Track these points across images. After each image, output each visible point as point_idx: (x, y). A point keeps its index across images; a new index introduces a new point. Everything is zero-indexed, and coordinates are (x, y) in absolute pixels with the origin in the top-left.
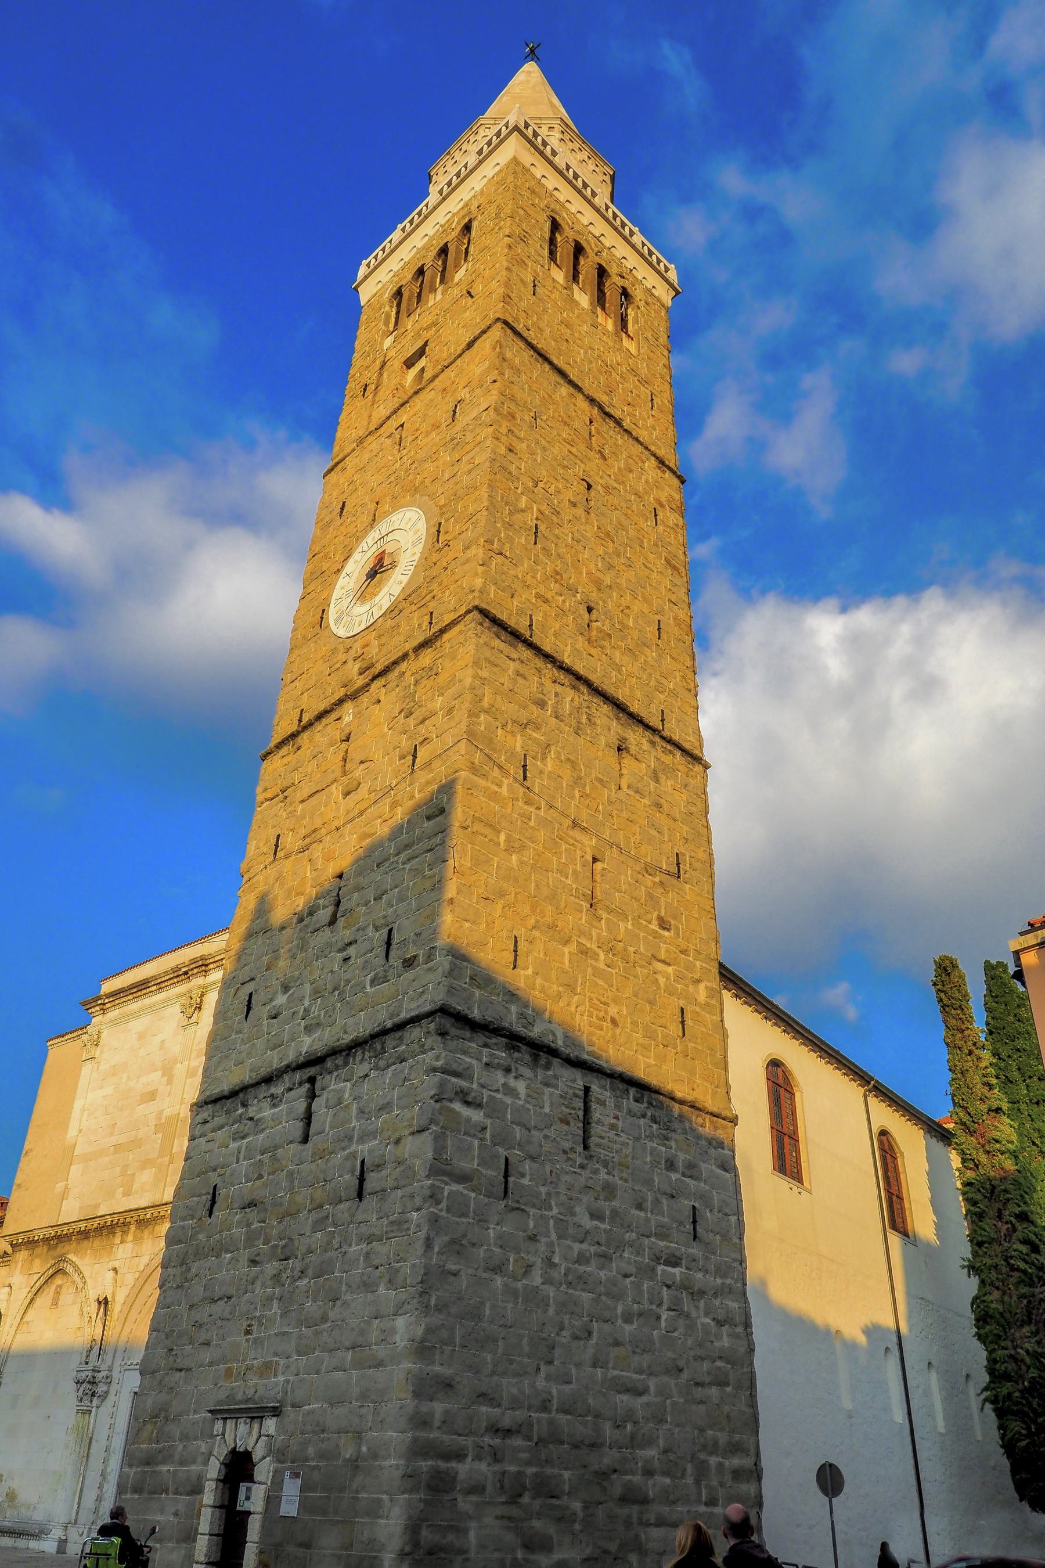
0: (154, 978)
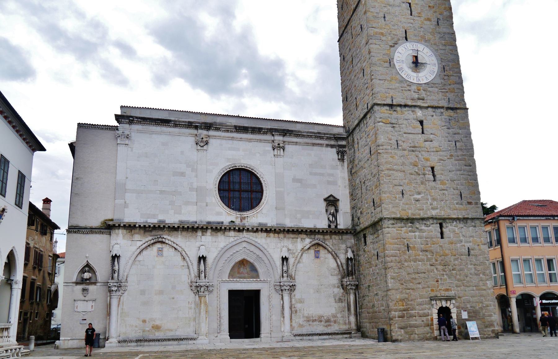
0: (175, 121)
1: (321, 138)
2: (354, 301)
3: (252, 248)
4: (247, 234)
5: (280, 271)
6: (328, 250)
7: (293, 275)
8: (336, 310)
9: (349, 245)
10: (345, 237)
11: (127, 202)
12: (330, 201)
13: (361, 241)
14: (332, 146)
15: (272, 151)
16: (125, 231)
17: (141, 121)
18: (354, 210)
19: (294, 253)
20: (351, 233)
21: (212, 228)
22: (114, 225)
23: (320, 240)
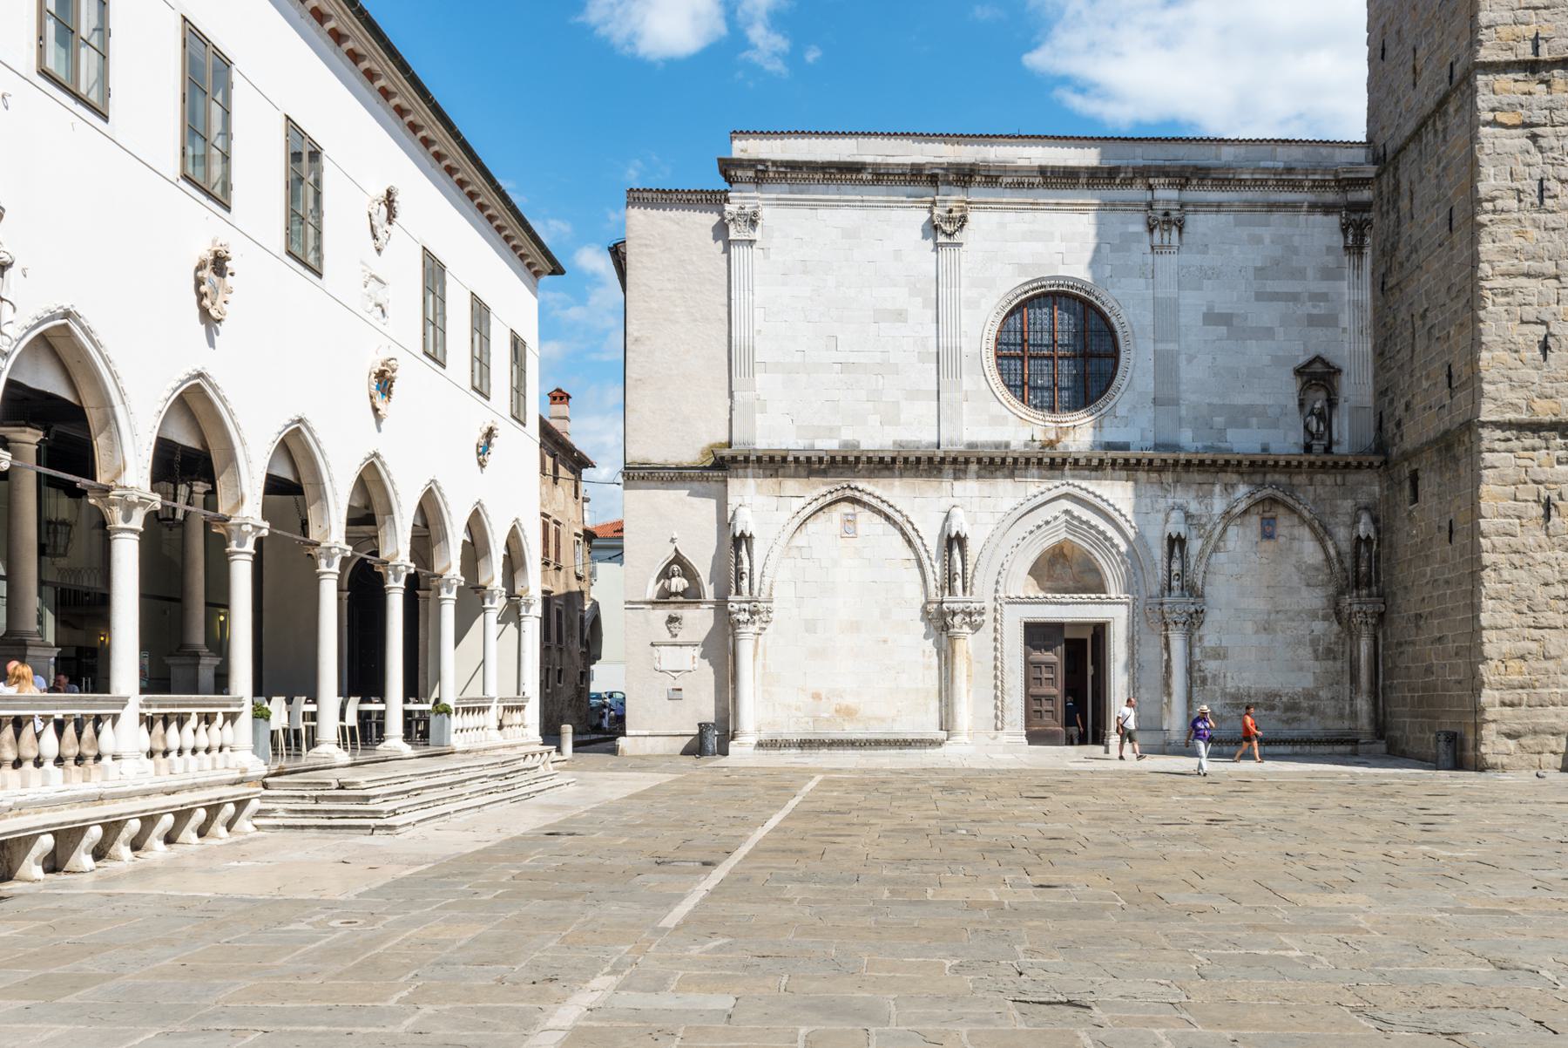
0: (876, 166)
1: (1294, 186)
2: (1369, 655)
3: (1086, 515)
4: (1074, 477)
5: (1161, 573)
6: (1301, 516)
7: (1199, 583)
8: (1316, 679)
9: (1363, 499)
10: (1352, 478)
11: (762, 398)
12: (1313, 375)
13: (1401, 490)
14: (1328, 209)
15: (1147, 235)
16: (761, 471)
17: (786, 173)
18: (1387, 400)
19: (1205, 525)
20: (1371, 466)
21: (979, 461)
22: (734, 459)
23: (1277, 489)
